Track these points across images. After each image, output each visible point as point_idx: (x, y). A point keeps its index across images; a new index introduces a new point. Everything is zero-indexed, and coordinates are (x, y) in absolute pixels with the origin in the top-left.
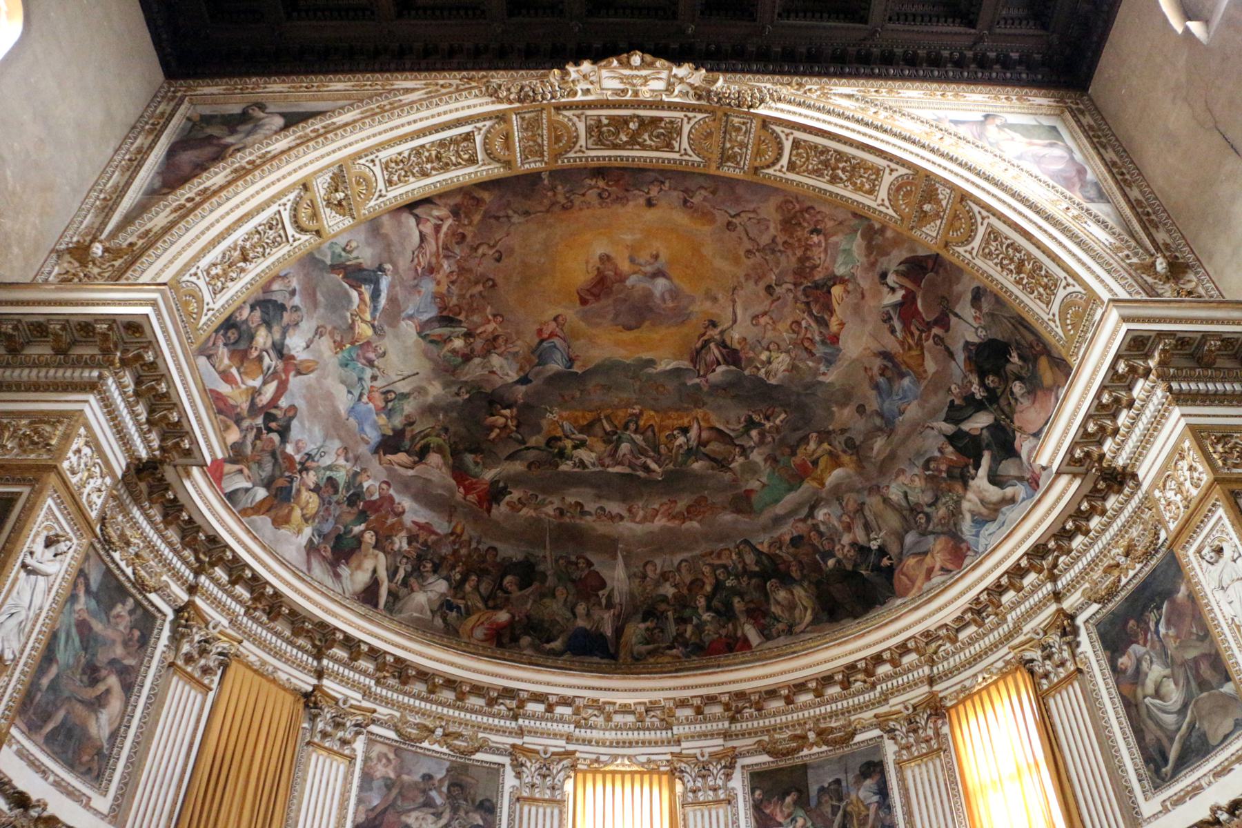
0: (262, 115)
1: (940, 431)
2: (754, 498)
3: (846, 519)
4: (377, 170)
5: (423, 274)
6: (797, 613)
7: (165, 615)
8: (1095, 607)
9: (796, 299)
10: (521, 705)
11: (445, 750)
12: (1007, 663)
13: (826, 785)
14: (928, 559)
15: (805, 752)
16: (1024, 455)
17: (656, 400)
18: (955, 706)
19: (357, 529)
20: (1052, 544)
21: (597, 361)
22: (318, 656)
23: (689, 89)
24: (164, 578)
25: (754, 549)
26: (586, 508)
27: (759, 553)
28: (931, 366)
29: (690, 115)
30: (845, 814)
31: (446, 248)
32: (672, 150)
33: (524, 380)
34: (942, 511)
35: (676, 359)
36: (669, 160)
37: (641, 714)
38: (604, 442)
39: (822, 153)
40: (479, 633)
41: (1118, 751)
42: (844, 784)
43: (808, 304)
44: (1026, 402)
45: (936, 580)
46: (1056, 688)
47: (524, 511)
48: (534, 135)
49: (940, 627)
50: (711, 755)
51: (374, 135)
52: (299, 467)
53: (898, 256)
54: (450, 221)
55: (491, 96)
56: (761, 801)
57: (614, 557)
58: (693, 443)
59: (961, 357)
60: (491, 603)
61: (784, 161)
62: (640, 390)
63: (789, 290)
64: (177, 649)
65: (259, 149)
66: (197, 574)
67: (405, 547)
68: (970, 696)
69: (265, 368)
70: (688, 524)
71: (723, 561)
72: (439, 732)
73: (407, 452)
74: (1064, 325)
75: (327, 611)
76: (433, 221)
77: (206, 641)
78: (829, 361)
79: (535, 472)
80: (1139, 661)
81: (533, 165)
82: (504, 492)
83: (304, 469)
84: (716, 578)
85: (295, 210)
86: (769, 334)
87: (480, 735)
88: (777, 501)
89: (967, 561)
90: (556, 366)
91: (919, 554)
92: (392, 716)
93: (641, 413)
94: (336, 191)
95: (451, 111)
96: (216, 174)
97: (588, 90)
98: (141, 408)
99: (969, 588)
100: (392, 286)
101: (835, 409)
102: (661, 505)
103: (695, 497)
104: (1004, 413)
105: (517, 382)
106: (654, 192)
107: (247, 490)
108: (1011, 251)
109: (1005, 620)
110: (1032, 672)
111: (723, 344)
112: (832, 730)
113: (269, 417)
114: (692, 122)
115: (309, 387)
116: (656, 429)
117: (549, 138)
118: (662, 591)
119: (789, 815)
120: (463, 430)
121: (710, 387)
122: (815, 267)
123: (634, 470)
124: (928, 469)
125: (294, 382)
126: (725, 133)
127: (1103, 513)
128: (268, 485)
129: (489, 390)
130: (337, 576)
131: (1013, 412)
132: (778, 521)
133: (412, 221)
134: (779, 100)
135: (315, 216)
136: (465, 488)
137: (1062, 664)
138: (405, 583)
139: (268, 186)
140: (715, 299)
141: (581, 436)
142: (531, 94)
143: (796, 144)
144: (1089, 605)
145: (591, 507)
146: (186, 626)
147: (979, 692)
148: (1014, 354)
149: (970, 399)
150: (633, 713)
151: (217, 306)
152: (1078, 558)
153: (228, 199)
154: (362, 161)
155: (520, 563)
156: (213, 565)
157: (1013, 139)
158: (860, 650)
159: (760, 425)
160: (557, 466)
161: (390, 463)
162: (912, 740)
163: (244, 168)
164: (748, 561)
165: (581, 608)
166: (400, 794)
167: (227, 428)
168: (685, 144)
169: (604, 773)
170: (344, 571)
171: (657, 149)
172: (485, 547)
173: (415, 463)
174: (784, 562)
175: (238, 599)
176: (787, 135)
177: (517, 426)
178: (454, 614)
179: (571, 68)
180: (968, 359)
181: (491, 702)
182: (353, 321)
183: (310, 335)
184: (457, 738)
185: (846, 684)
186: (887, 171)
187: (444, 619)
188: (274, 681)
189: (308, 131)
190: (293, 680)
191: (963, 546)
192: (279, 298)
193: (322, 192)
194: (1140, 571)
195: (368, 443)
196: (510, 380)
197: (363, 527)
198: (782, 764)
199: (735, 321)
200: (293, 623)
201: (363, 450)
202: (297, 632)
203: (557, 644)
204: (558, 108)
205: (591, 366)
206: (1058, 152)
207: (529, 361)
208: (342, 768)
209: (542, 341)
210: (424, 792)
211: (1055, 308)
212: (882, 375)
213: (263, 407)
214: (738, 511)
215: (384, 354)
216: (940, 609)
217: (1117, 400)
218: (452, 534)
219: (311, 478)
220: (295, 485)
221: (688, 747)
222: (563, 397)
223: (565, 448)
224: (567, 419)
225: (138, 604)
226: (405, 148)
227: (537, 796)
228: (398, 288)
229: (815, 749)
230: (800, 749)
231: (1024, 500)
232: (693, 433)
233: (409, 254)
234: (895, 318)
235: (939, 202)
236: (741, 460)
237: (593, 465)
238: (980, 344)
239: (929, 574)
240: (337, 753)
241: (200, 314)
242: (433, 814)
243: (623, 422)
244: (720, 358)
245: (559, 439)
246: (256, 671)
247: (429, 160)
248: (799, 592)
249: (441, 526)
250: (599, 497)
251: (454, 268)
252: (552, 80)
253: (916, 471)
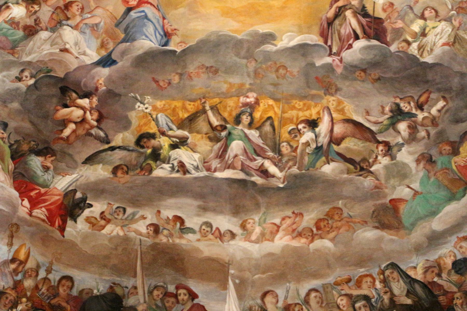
2: (403, 209)
17: (275, 85)
21: (201, 36)
26: (188, 224)
27: (411, 281)
35: (301, 32)
38: (210, 139)
47: (109, 229)
57: (225, 287)
58: (324, 140)
62: (256, 73)
70: (318, 244)
71: (364, 291)
79: (123, 178)
88: (434, 213)
93: (257, 102)
102: (283, 219)
103: (326, 208)
116: (276, 124)
120: (27, 126)
121: (345, 68)
123: (247, 174)
129: (62, 75)
136: (30, 202)
141: (180, 133)
155: (102, 297)
159: (410, 115)
160: (151, 171)
164: (396, 291)
172: (58, 278)
174: (446, 293)
177: (98, 121)
196: (88, 61)
205: (192, 42)
207: (113, 36)
209: (129, 10)
214: (382, 226)
218: (13, 260)
222: (157, 82)
223: (161, 148)
224: (163, 110)
232: (323, 127)
236: (385, 161)
237: (197, 168)
243: (234, 114)
244: (359, 31)
245: (153, 136)
250: (204, 209)
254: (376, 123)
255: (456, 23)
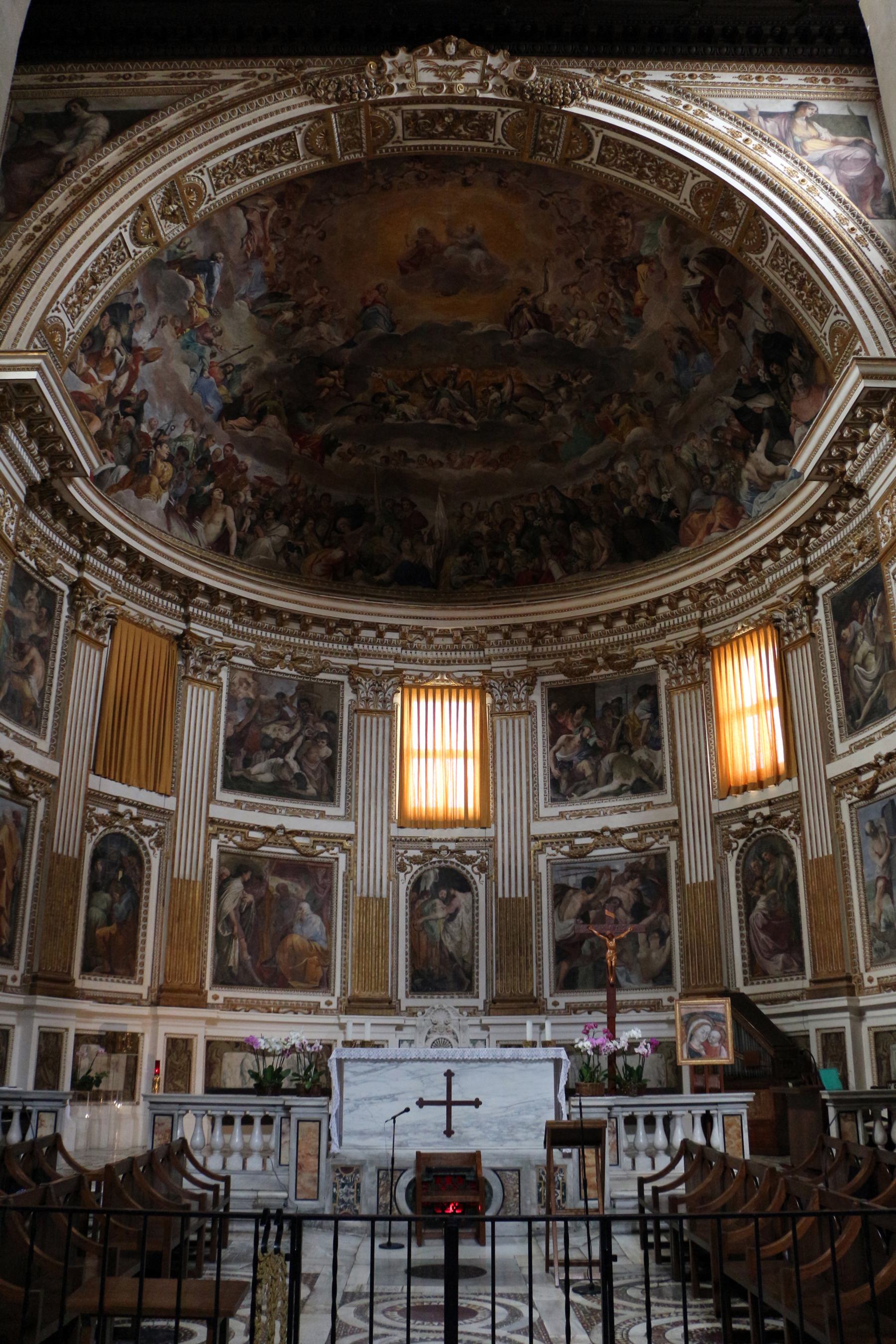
0: (86, 114)
1: (728, 404)
3: (641, 472)
4: (206, 178)
5: (252, 258)
6: (595, 551)
7: (63, 591)
8: (832, 584)
9: (604, 273)
10: (356, 632)
11: (293, 672)
12: (762, 617)
13: (610, 702)
14: (710, 517)
15: (595, 673)
16: (796, 440)
18: (718, 647)
19: (207, 488)
20: (804, 529)
22: (185, 605)
23: (502, 82)
24: (59, 561)
25: (559, 494)
27: (564, 498)
28: (724, 346)
29: (504, 109)
30: (623, 725)
31: (272, 232)
32: (486, 139)
33: (350, 344)
34: (724, 476)
36: (484, 149)
37: (457, 638)
39: (630, 151)
40: (318, 569)
41: (829, 703)
42: (624, 702)
43: (614, 278)
44: (801, 394)
45: (715, 535)
46: (794, 645)
47: (354, 460)
48: (352, 130)
49: (712, 581)
50: (516, 673)
51: (200, 146)
52: (153, 442)
53: (697, 246)
54: (275, 208)
55: (309, 94)
56: (556, 712)
58: (506, 397)
59: (750, 343)
60: (327, 543)
61: (594, 155)
63: (597, 264)
64: (77, 618)
65: (92, 164)
66: (83, 553)
67: (250, 499)
68: (730, 641)
69: (117, 362)
70: (500, 471)
72: (288, 658)
73: (246, 416)
74: (832, 347)
75: (189, 568)
76: (259, 210)
77: (98, 608)
78: (633, 331)
80: (856, 635)
81: (352, 156)
82: (335, 444)
83: (158, 443)
84: (525, 518)
85: (135, 229)
86: (578, 303)
87: (323, 658)
89: (741, 523)
90: (380, 329)
91: (703, 510)
92: (249, 647)
93: (459, 371)
94: (170, 203)
95: (272, 114)
96: (56, 196)
97: (404, 85)
98: (33, 446)
99: (736, 553)
100: (224, 272)
101: (636, 374)
104: (783, 399)
105: (343, 346)
106: (470, 173)
107: (112, 470)
108: (795, 269)
109: (764, 582)
110: (778, 629)
111: (534, 310)
112: (617, 657)
113: (124, 404)
114: (506, 116)
115: (156, 372)
117: (367, 130)
118: (477, 529)
119: (578, 725)
122: (622, 246)
124: (716, 437)
125: (144, 370)
126: (537, 126)
127: (846, 510)
128: (128, 462)
130: (193, 531)
131: (791, 399)
132: (582, 470)
133: (240, 213)
134: (592, 95)
135: (153, 229)
136: (300, 443)
137: (801, 627)
138: (251, 530)
139: (108, 212)
140: (528, 269)
142: (348, 93)
143: (606, 141)
144: (828, 582)
145: (413, 455)
146: (80, 600)
147: (738, 638)
148: (796, 350)
149: (756, 380)
150: (451, 636)
151: (75, 330)
152: (823, 543)
153: (74, 230)
154: (191, 173)
156: (94, 545)
157: (818, 137)
158: (644, 593)
159: (568, 384)
160: (383, 419)
161: (232, 427)
162: (680, 672)
163: (80, 188)
164: (553, 504)
165: (406, 544)
166: (260, 711)
167: (90, 420)
168: (499, 135)
169: (427, 688)
170: (199, 526)
171: (472, 139)
173: (254, 425)
175: (117, 568)
176: (597, 132)
178: (295, 554)
179: (387, 60)
180: (757, 346)
181: (330, 631)
182: (191, 308)
183: (154, 327)
184: (303, 662)
185: (631, 620)
186: (690, 175)
187: (287, 559)
188: (152, 630)
189: (135, 138)
190: (166, 626)
191: (739, 508)
192: (124, 300)
193: (157, 207)
194: (867, 563)
195: (209, 411)
197: (211, 486)
198: (575, 682)
199: (546, 289)
200: (161, 579)
201: (208, 419)
202: (165, 587)
203: (385, 576)
204: (376, 105)
206: (861, 153)
208: (212, 694)
209: (366, 308)
210: (279, 708)
211: (827, 329)
212: (680, 348)
213: (119, 396)
215: (221, 332)
216: (712, 567)
217: (855, 436)
218: (290, 484)
219: (164, 450)
220: (151, 458)
221: (498, 666)
225: (42, 586)
226: (230, 154)
227: (372, 708)
228: (230, 272)
229: (603, 672)
230: (590, 670)
231: (792, 479)
232: (507, 389)
233: (238, 241)
234: (694, 300)
235: (735, 211)
236: (550, 414)
237: (415, 417)
238: (767, 336)
239: (708, 532)
240: (207, 683)
241: (63, 342)
242: (287, 725)
244: (532, 322)
245: (383, 395)
246: (137, 624)
247: (253, 161)
248: (598, 534)
249: (280, 478)
251: (281, 249)
252: (369, 75)
253: (705, 437)
254: (543, 387)
255: (600, 323)
